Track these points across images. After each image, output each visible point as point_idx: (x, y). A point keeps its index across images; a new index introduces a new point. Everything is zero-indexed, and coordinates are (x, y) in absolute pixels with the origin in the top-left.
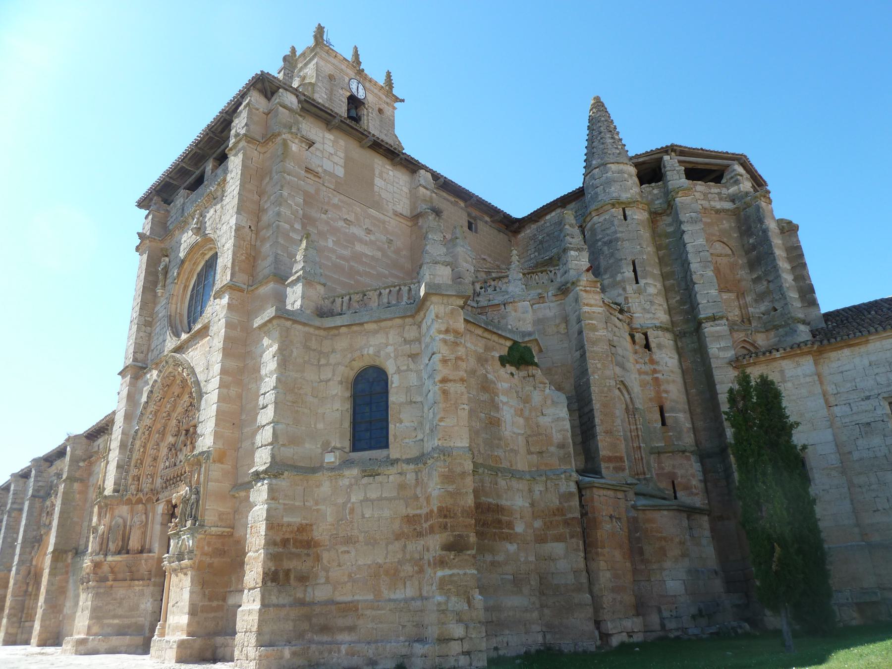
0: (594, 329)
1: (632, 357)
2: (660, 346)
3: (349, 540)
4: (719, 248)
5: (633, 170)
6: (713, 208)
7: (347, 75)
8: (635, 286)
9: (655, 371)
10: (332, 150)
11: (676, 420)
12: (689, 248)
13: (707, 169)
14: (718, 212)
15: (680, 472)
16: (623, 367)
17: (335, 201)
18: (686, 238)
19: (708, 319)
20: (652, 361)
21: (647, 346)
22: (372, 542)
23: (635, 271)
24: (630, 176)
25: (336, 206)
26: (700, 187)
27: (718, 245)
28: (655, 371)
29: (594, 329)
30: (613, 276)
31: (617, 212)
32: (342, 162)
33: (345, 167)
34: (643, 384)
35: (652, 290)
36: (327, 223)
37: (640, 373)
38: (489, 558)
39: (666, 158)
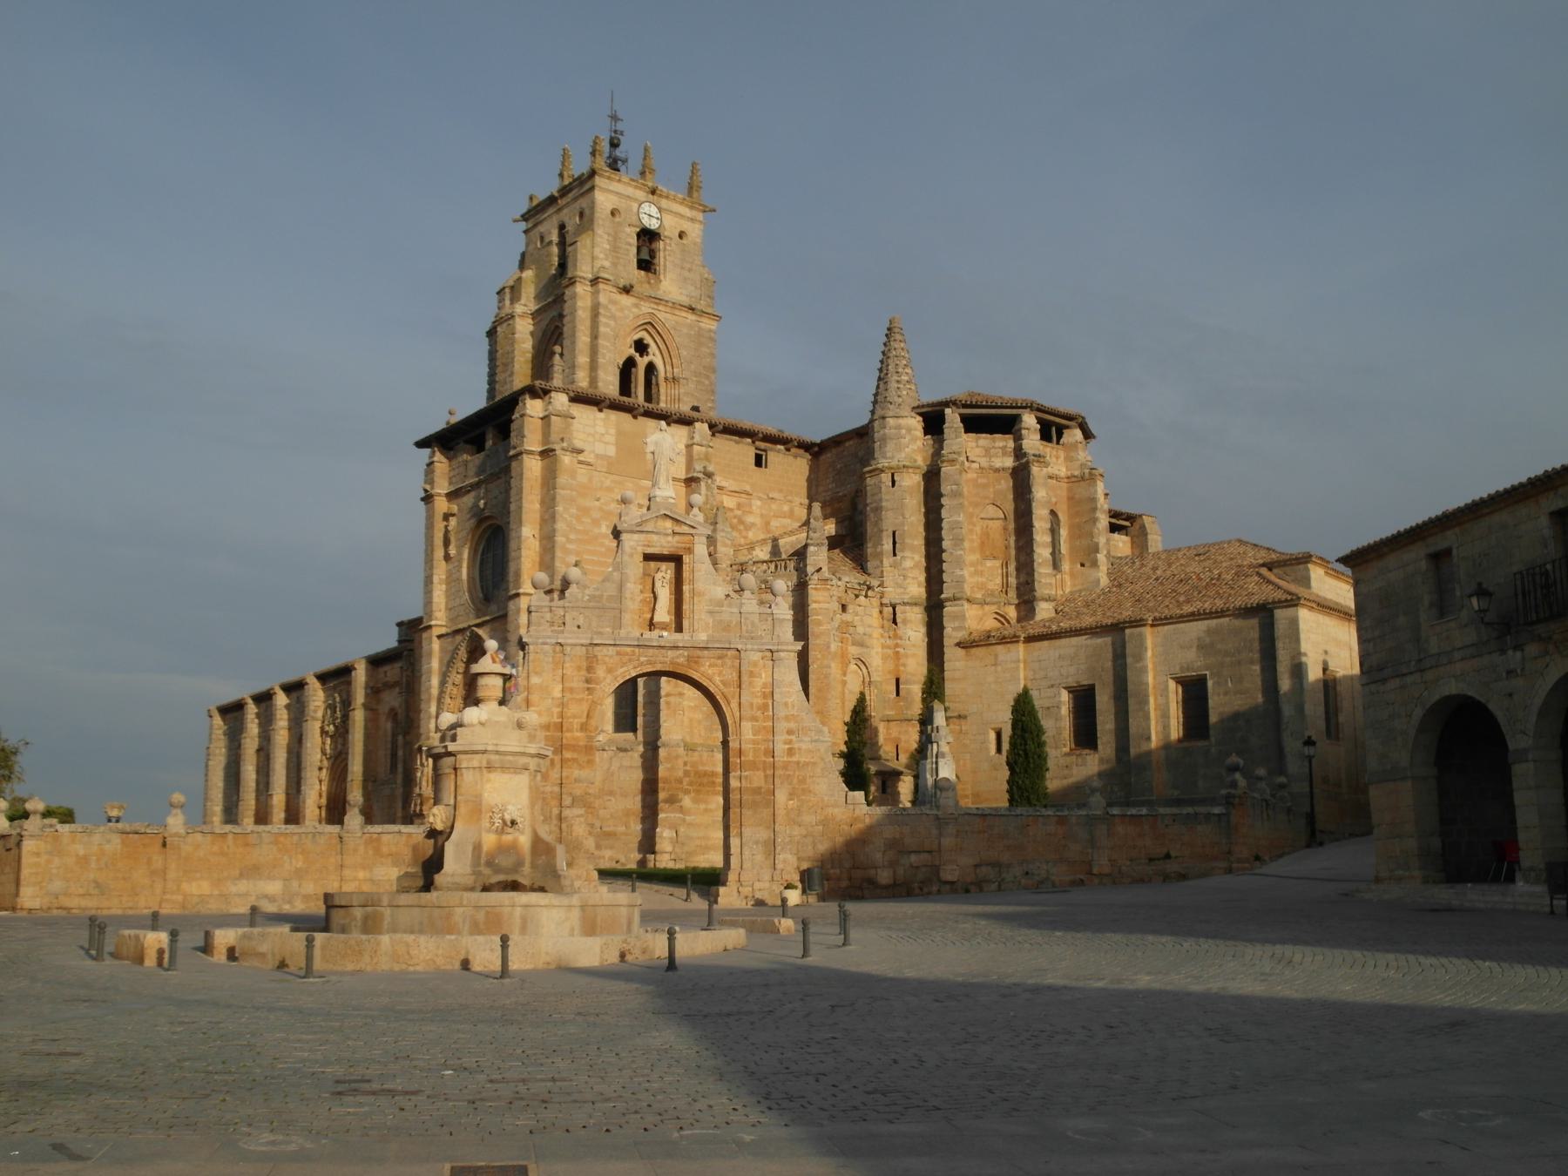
0: (819, 623)
1: (877, 633)
2: (905, 622)
3: (611, 793)
4: (992, 511)
5: (916, 423)
6: (991, 468)
7: (636, 200)
8: (892, 559)
9: (897, 645)
10: (601, 430)
11: (909, 692)
12: (944, 525)
13: (991, 420)
14: (997, 470)
15: (903, 738)
16: (861, 644)
17: (608, 483)
18: (944, 513)
19: (948, 600)
20: (896, 636)
21: (895, 622)
22: (625, 795)
23: (894, 543)
24: (909, 430)
25: (609, 489)
26: (984, 440)
27: (991, 509)
28: (897, 645)
29: (819, 623)
30: (875, 546)
31: (886, 478)
32: (612, 439)
33: (617, 444)
34: (885, 658)
35: (908, 564)
36: (601, 509)
37: (883, 647)
38: (702, 806)
39: (948, 411)
